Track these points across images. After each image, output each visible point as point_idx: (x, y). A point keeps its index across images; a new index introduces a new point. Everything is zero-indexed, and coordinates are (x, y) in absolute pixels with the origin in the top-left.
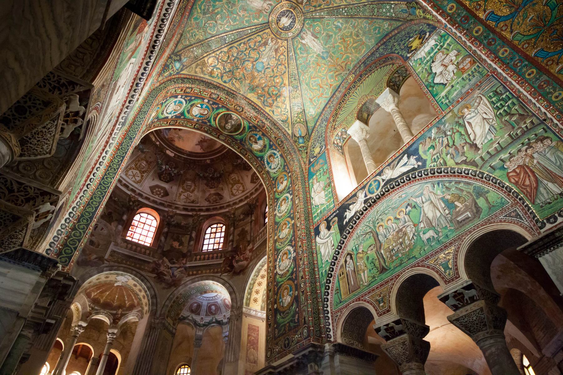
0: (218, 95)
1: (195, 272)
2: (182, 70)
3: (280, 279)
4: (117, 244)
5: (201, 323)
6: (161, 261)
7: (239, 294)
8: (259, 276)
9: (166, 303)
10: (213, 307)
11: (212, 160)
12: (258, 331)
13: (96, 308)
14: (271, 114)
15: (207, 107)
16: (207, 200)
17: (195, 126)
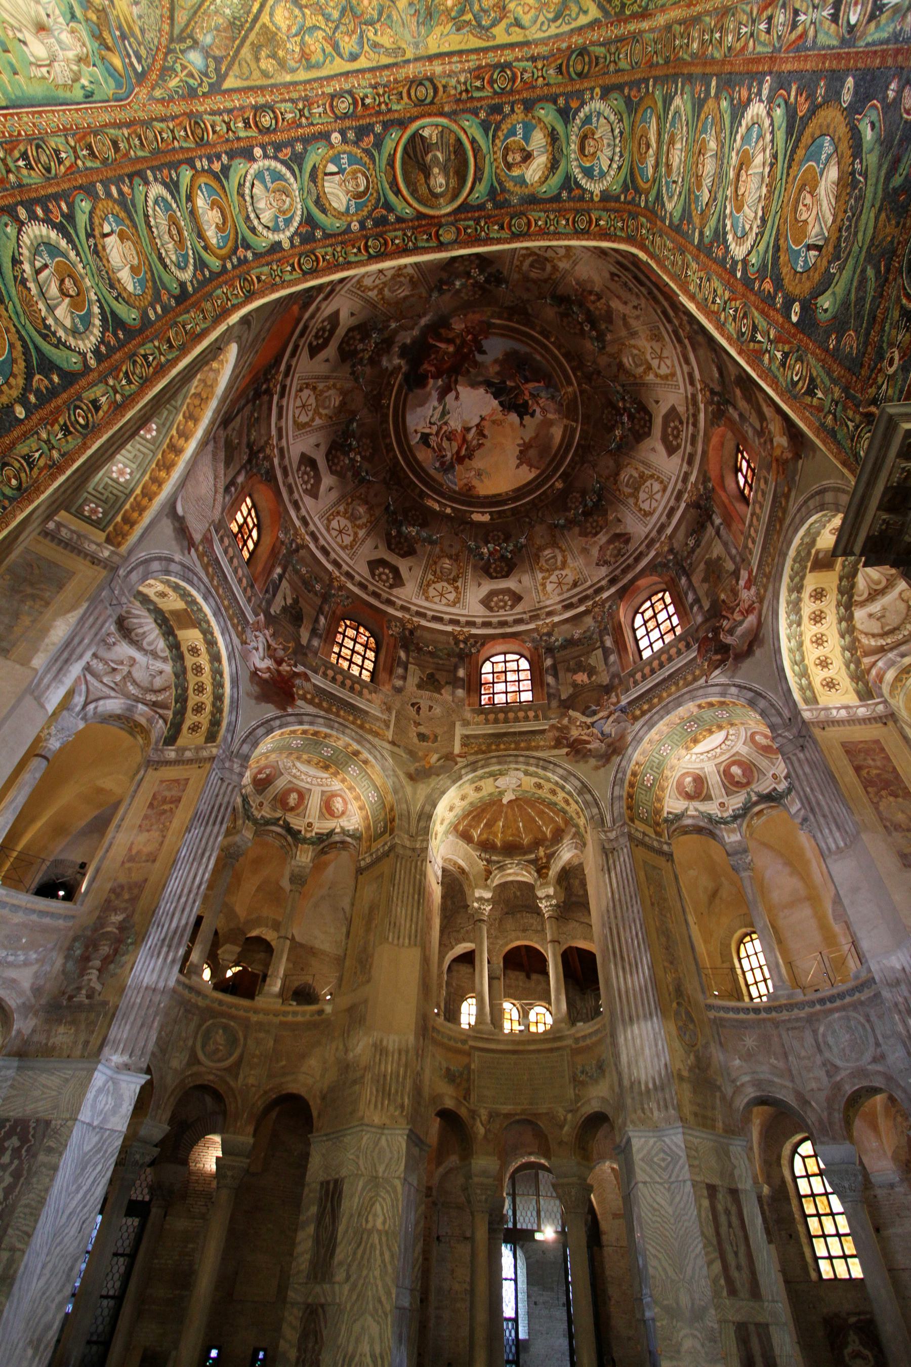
0: (350, 93)
1: (646, 707)
2: (222, 78)
3: (762, 247)
4: (466, 723)
5: (725, 815)
6: (565, 721)
7: (776, 694)
8: (805, 619)
9: (616, 793)
10: (736, 770)
11: (565, 476)
12: (883, 750)
13: (494, 858)
14: (517, 36)
15: (353, 160)
16: (600, 563)
17: (367, 247)
